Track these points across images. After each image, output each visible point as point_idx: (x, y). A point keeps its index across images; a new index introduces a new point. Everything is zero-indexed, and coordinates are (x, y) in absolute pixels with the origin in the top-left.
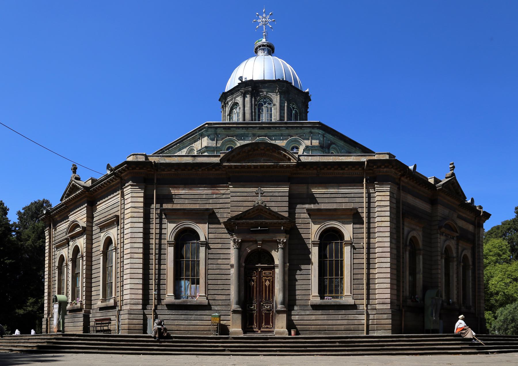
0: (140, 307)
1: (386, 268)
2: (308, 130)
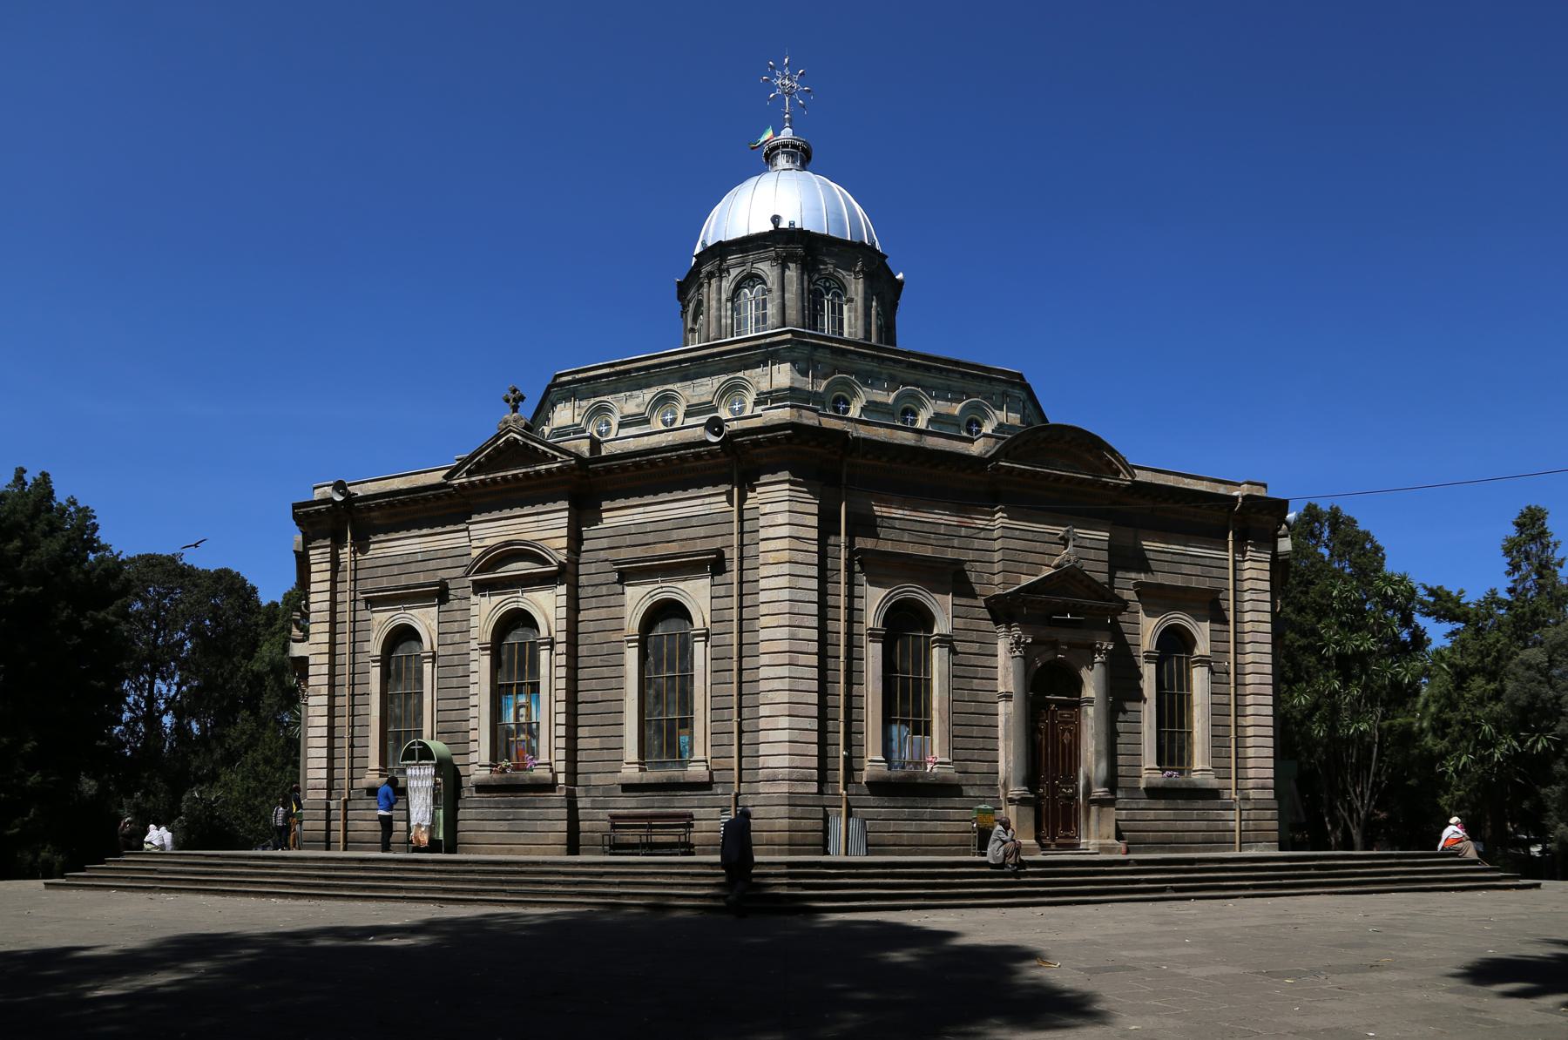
0: (814, 788)
2: (1002, 388)
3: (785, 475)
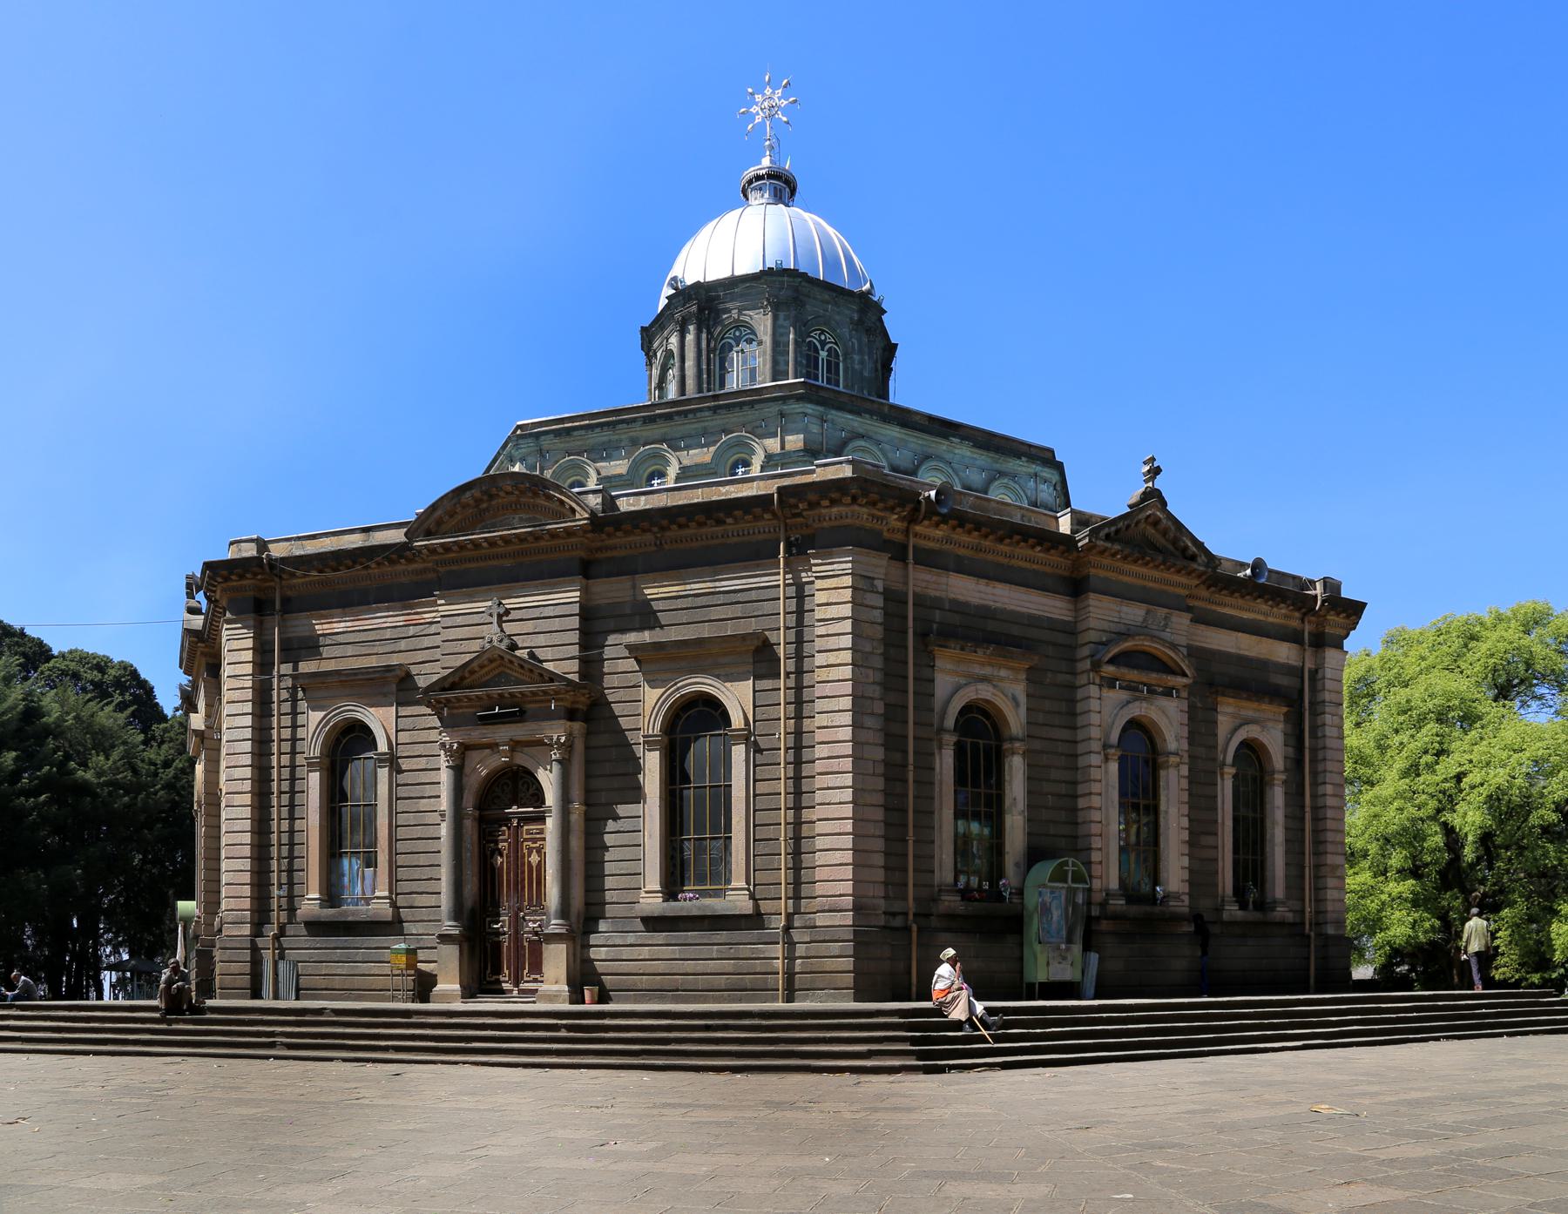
1: (840, 803)
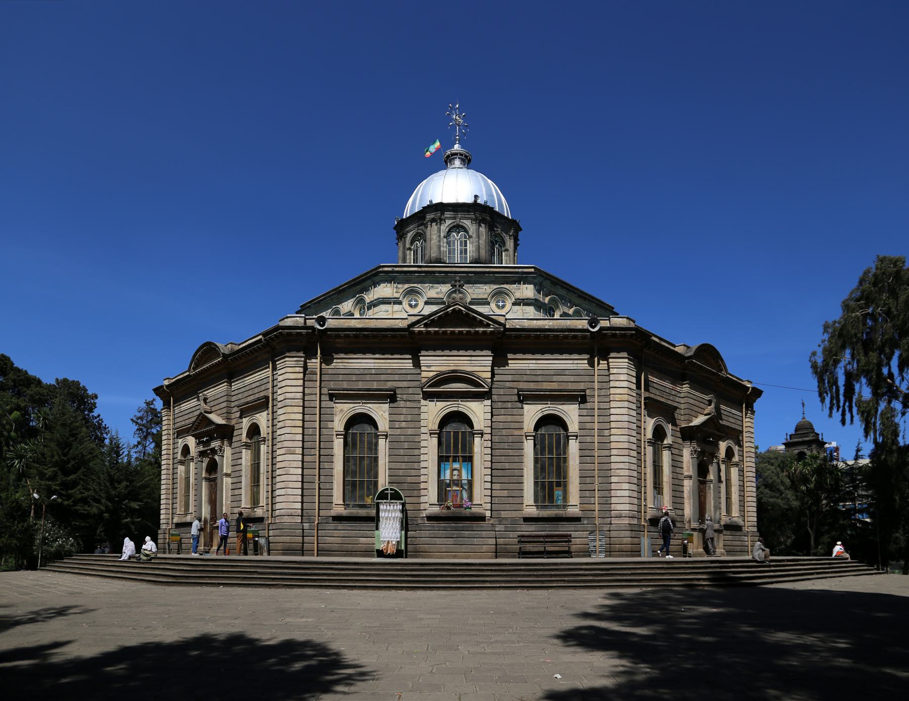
3: (625, 354)
